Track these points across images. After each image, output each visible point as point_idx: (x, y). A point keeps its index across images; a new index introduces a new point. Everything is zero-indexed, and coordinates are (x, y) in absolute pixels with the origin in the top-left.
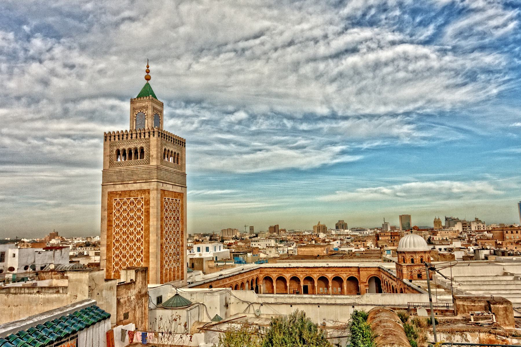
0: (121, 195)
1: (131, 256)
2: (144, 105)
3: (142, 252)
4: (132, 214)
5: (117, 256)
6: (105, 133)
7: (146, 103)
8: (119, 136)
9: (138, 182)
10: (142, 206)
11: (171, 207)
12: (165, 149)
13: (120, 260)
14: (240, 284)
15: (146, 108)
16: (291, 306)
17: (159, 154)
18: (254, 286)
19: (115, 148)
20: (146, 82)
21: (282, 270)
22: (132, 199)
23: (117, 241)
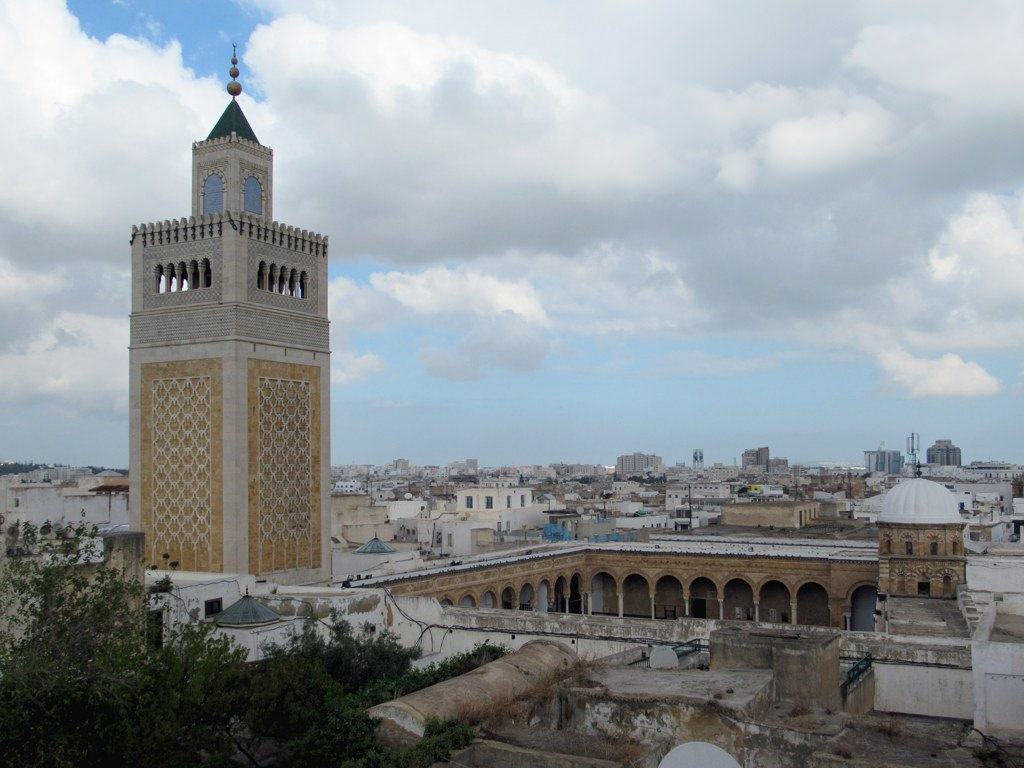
0: (165, 371)
1: (188, 510)
2: (219, 157)
3: (208, 500)
4: (188, 416)
5: (161, 509)
6: (135, 228)
7: (231, 152)
8: (160, 233)
9: (198, 340)
10: (207, 397)
11: (280, 400)
12: (262, 264)
13: (168, 517)
14: (517, 587)
15: (225, 163)
16: (513, 637)
17: (245, 277)
18: (567, 594)
19: (154, 264)
20: (229, 99)
21: (640, 557)
22: (188, 380)
23: (161, 475)
